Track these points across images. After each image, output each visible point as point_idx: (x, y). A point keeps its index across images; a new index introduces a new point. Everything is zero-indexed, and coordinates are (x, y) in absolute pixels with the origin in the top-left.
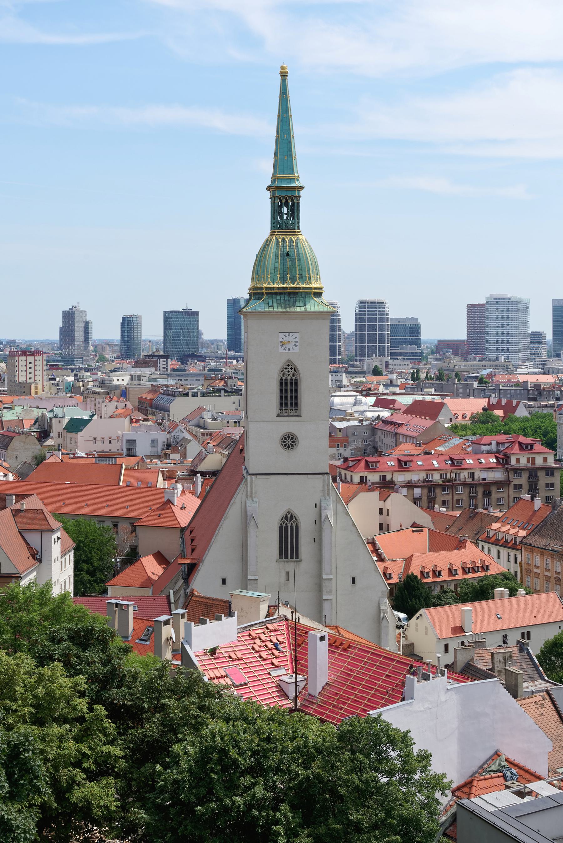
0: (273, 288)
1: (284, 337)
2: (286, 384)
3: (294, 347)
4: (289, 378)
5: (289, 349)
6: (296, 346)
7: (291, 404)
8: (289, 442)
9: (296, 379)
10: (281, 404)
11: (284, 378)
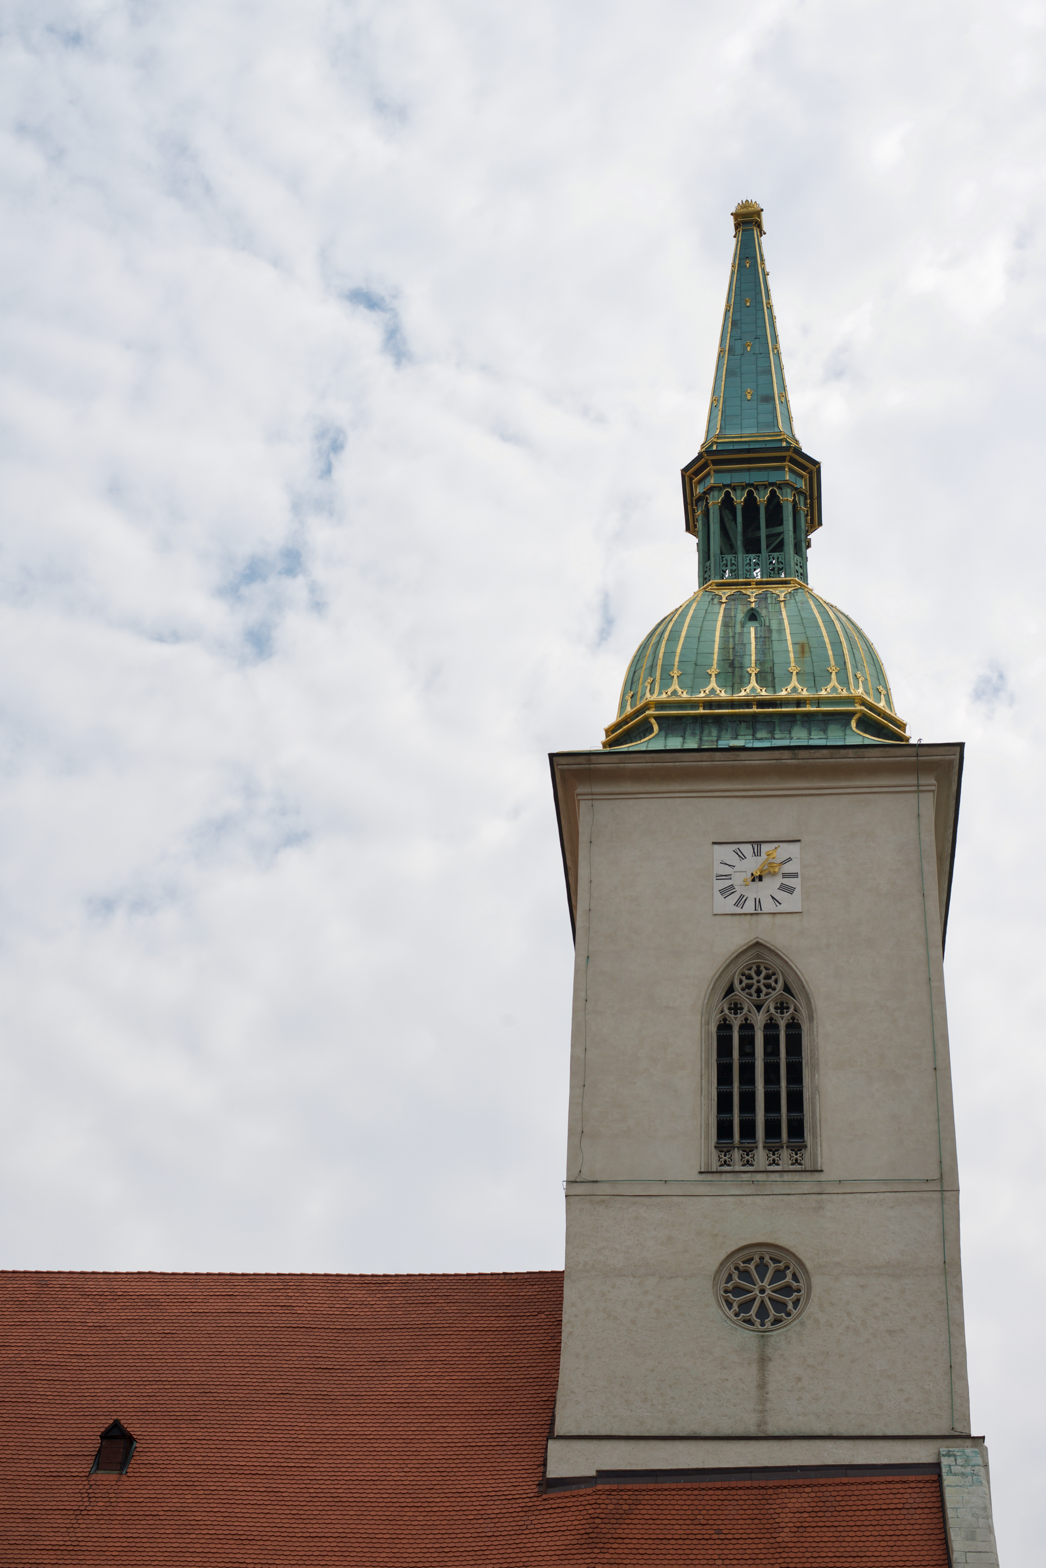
0: (694, 705)
1: (734, 859)
2: (748, 1040)
3: (781, 895)
4: (759, 1020)
5: (758, 903)
6: (790, 890)
7: (772, 1129)
8: (763, 1289)
10: (724, 1130)
11: (736, 1023)
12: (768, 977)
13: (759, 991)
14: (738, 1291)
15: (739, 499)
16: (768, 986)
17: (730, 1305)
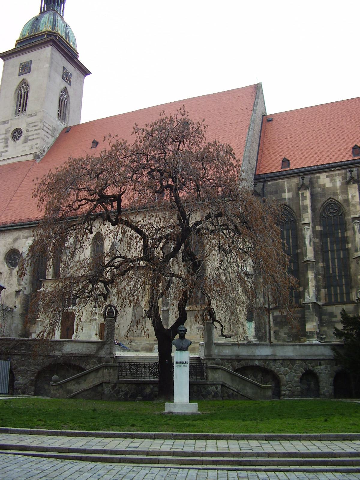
4: (23, 91)
9: (28, 92)
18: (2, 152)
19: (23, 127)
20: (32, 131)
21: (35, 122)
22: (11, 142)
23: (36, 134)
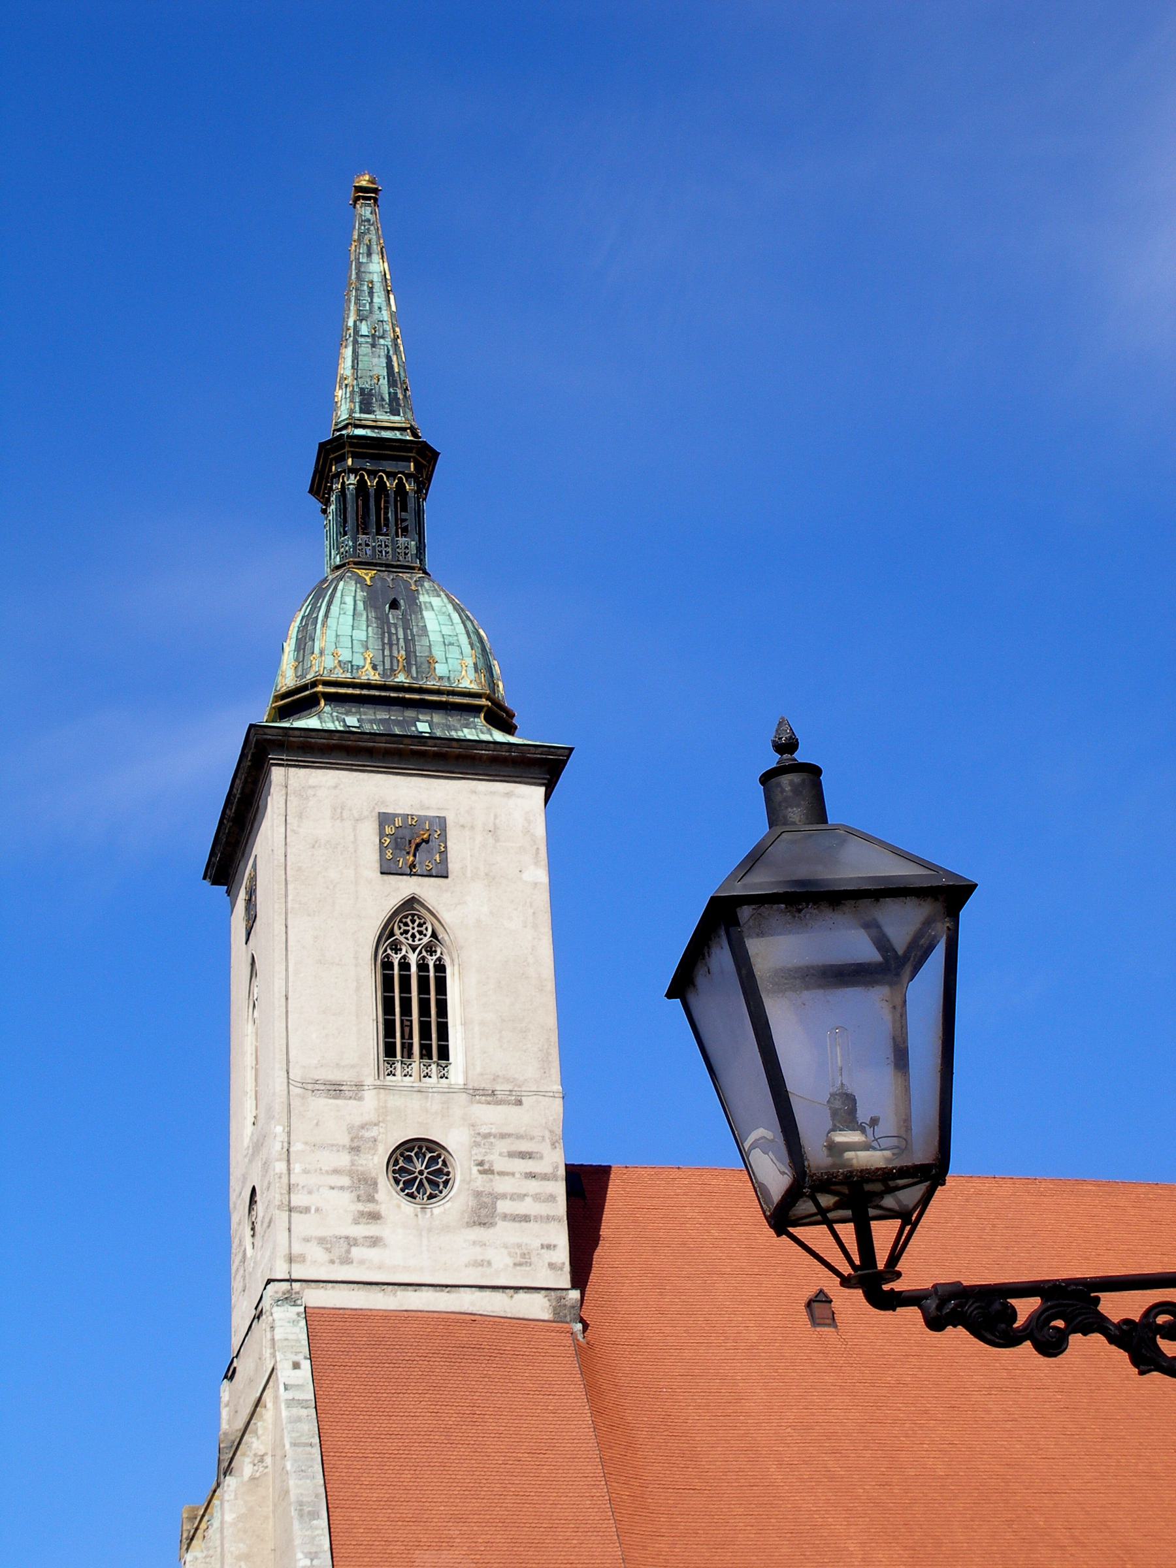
4: (413, 959)
9: (440, 968)
12: (420, 925)
13: (413, 936)
14: (403, 1170)
15: (372, 483)
16: (420, 933)
17: (397, 1182)
18: (352, 1242)
19: (455, 1141)
20: (513, 1174)
21: (519, 1137)
22: (388, 1195)
23: (537, 1198)
